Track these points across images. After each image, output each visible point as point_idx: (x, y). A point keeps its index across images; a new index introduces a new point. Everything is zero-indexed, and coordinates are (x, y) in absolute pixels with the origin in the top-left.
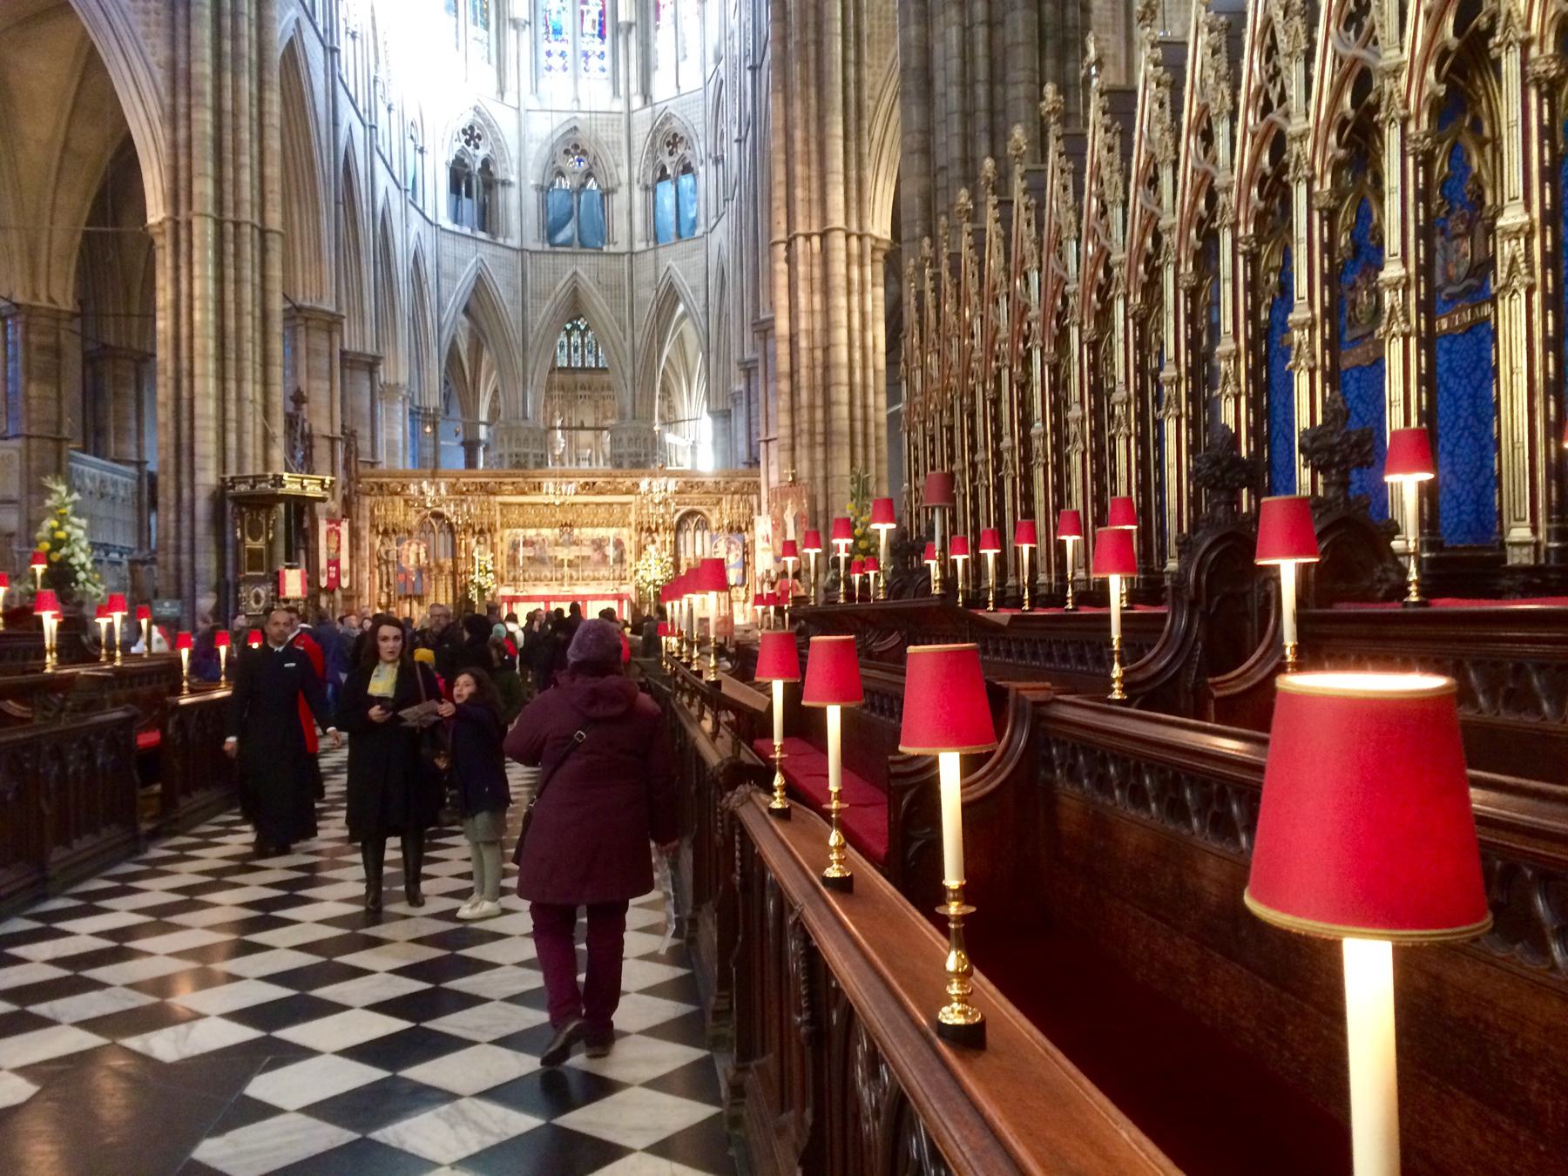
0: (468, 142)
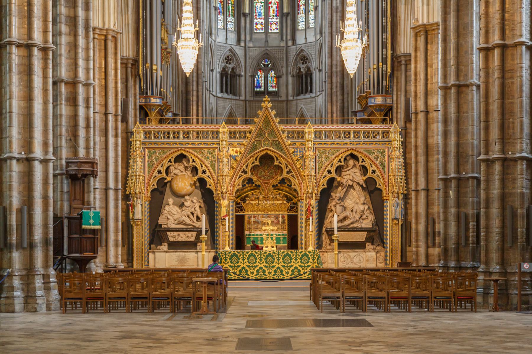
0: (227, 63)
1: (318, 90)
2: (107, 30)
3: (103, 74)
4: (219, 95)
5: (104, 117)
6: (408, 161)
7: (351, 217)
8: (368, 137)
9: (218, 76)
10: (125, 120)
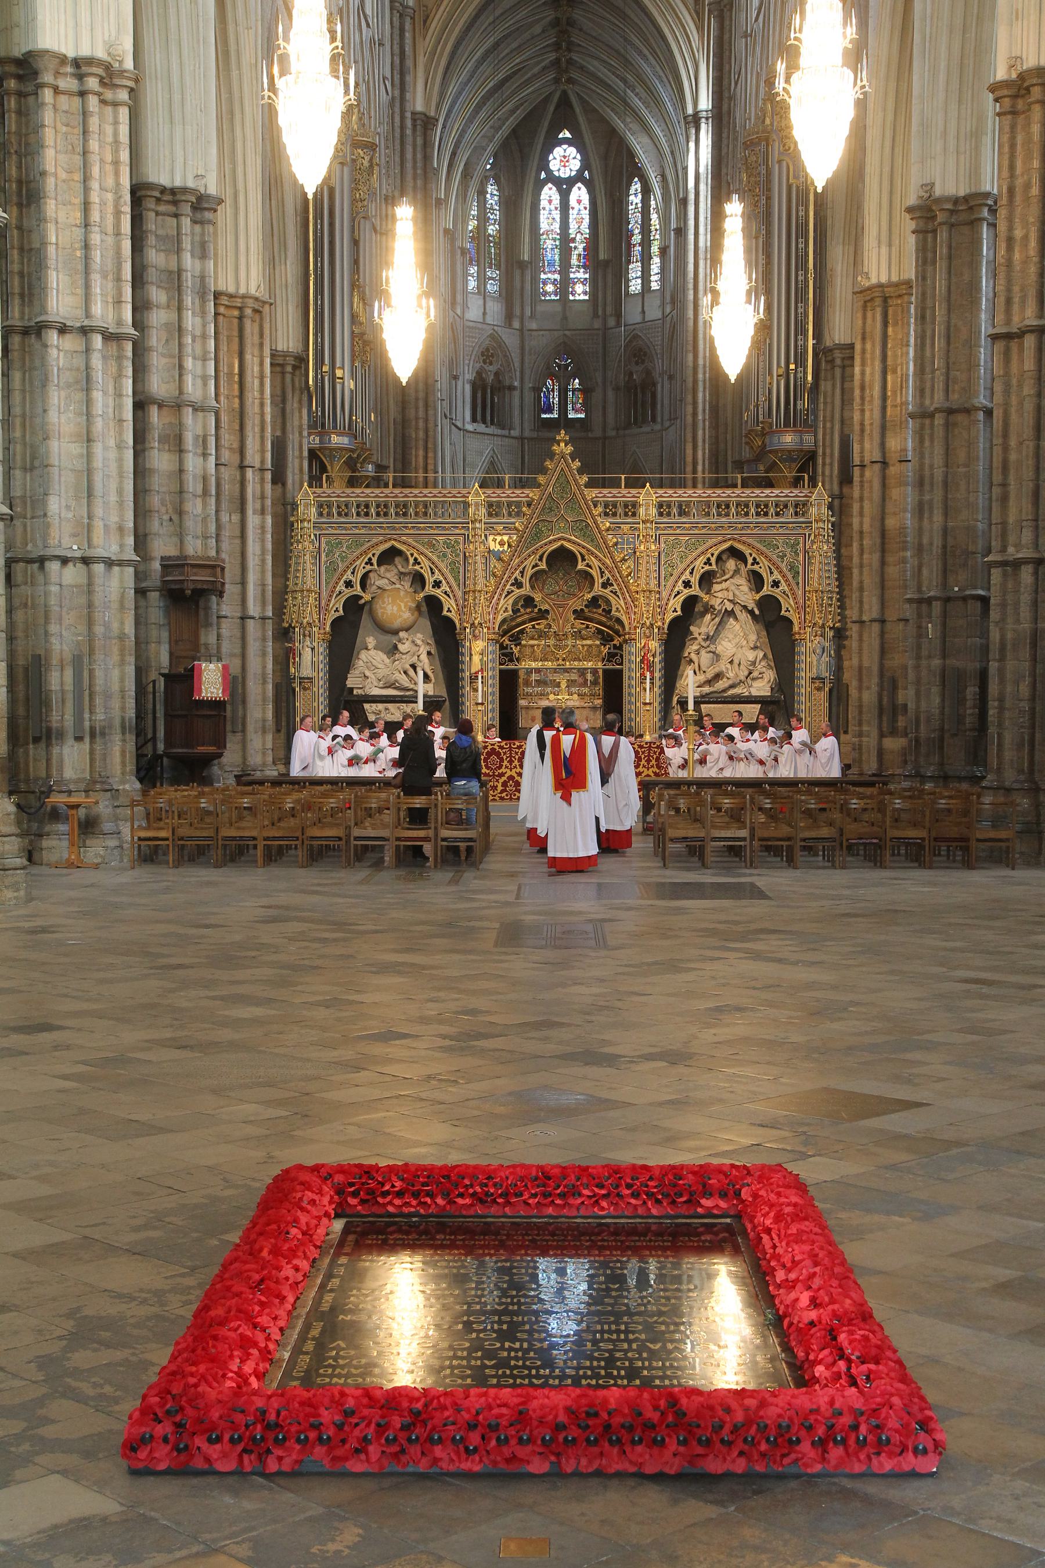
0: (484, 362)
1: (666, 417)
2: (244, 297)
3: (236, 386)
4: (470, 427)
5: (238, 473)
6: (845, 563)
7: (731, 675)
8: (766, 514)
9: (468, 388)
10: (279, 478)
